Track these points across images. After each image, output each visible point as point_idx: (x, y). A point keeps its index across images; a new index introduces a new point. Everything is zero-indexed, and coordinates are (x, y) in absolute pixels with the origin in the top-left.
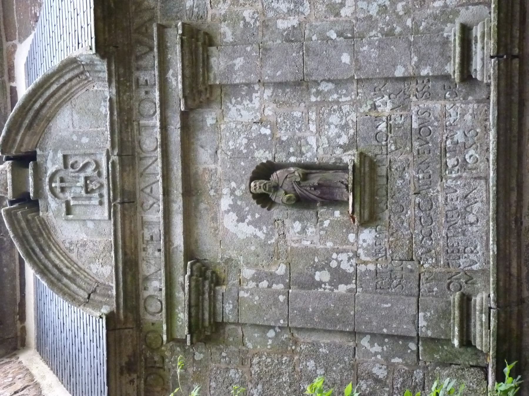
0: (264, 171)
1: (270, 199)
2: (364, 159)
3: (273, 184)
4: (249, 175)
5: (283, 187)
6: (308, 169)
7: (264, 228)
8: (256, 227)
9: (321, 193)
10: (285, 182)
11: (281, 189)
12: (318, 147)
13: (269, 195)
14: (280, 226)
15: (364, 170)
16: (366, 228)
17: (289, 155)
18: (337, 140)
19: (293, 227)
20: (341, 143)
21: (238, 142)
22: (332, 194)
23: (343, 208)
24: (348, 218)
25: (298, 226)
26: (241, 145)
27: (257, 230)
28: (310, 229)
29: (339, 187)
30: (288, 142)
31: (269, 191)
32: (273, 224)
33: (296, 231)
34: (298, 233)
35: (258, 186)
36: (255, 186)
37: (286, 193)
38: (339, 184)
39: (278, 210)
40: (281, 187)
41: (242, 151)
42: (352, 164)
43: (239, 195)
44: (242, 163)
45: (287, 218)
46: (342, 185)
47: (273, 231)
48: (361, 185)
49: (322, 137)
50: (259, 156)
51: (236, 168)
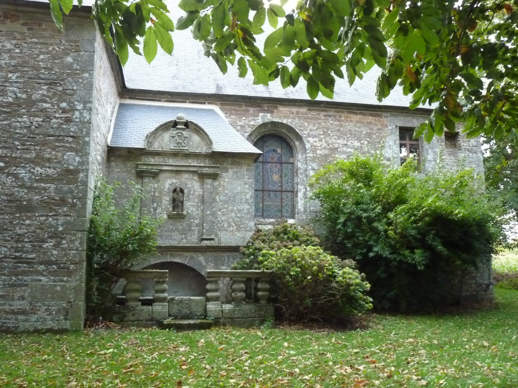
0: (182, 191)
6: (182, 202)
25: (168, 199)
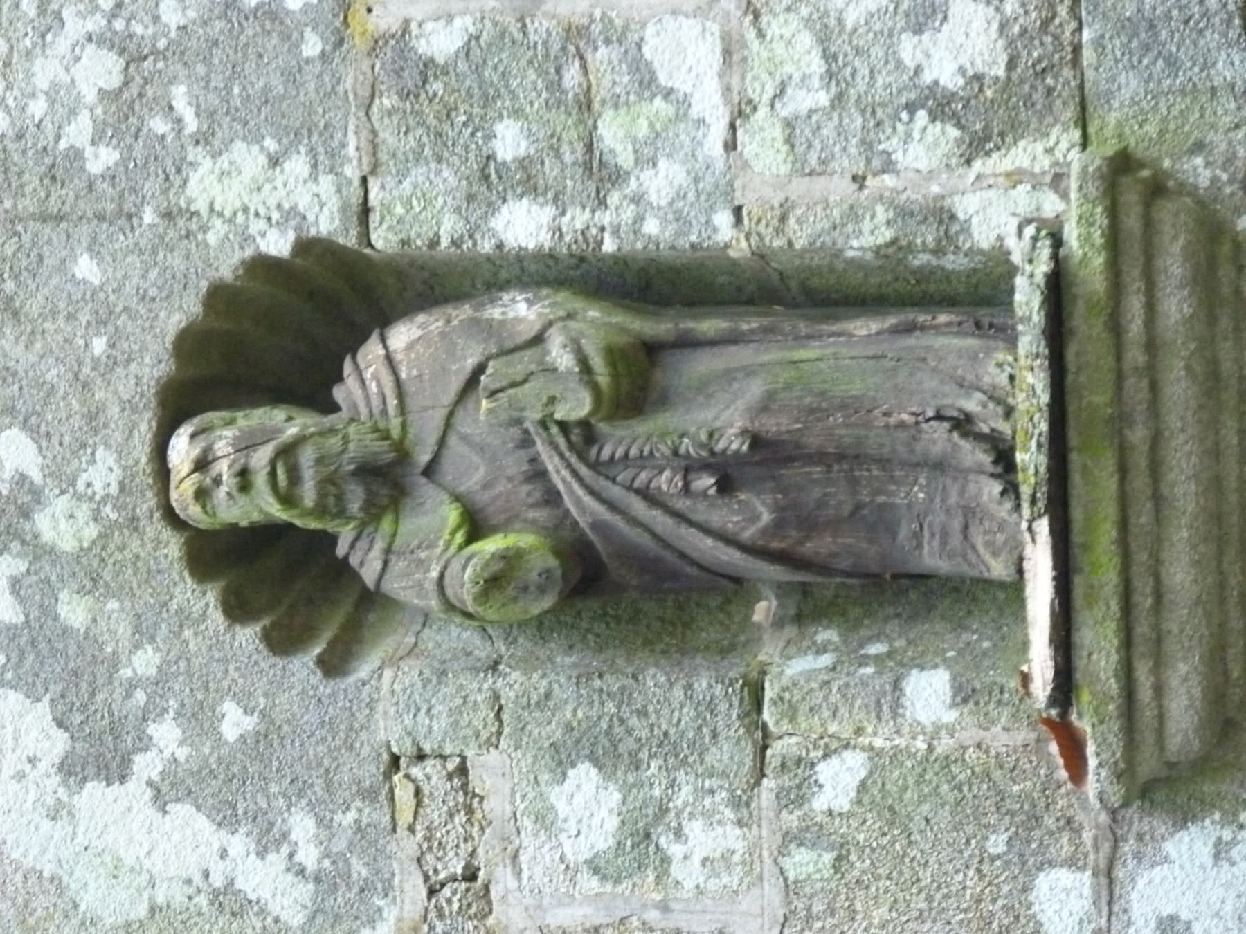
0: (280, 332)
1: (343, 571)
2: (1148, 223)
3: (360, 443)
4: (153, 364)
5: (448, 470)
6: (663, 303)
7: (302, 826)
8: (227, 819)
9: (778, 526)
10: (464, 425)
11: (427, 491)
12: (740, 113)
13: (332, 540)
14: (434, 812)
15: (1151, 307)
16: (1184, 818)
17: (490, 182)
18: (909, 48)
19: (545, 820)
20: (944, 72)
21: (42, 82)
22: (881, 522)
23: (979, 637)
24: (1024, 735)
25: (589, 805)
26: (63, 101)
27: (239, 844)
28: (694, 828)
29: (940, 466)
30: (478, 70)
31: (321, 510)
32: (378, 793)
33: (578, 851)
34: (594, 867)
35: (223, 468)
36: (202, 465)
37: (476, 526)
38: (938, 437)
39: (411, 672)
40: (429, 471)
41: (76, 155)
42: (1043, 267)
43: (67, 545)
44: (86, 268)
45: (493, 742)
46: (966, 445)
47: (376, 856)
48: (1123, 452)
49: (775, 26)
50: (229, 197)
51: (34, 307)
